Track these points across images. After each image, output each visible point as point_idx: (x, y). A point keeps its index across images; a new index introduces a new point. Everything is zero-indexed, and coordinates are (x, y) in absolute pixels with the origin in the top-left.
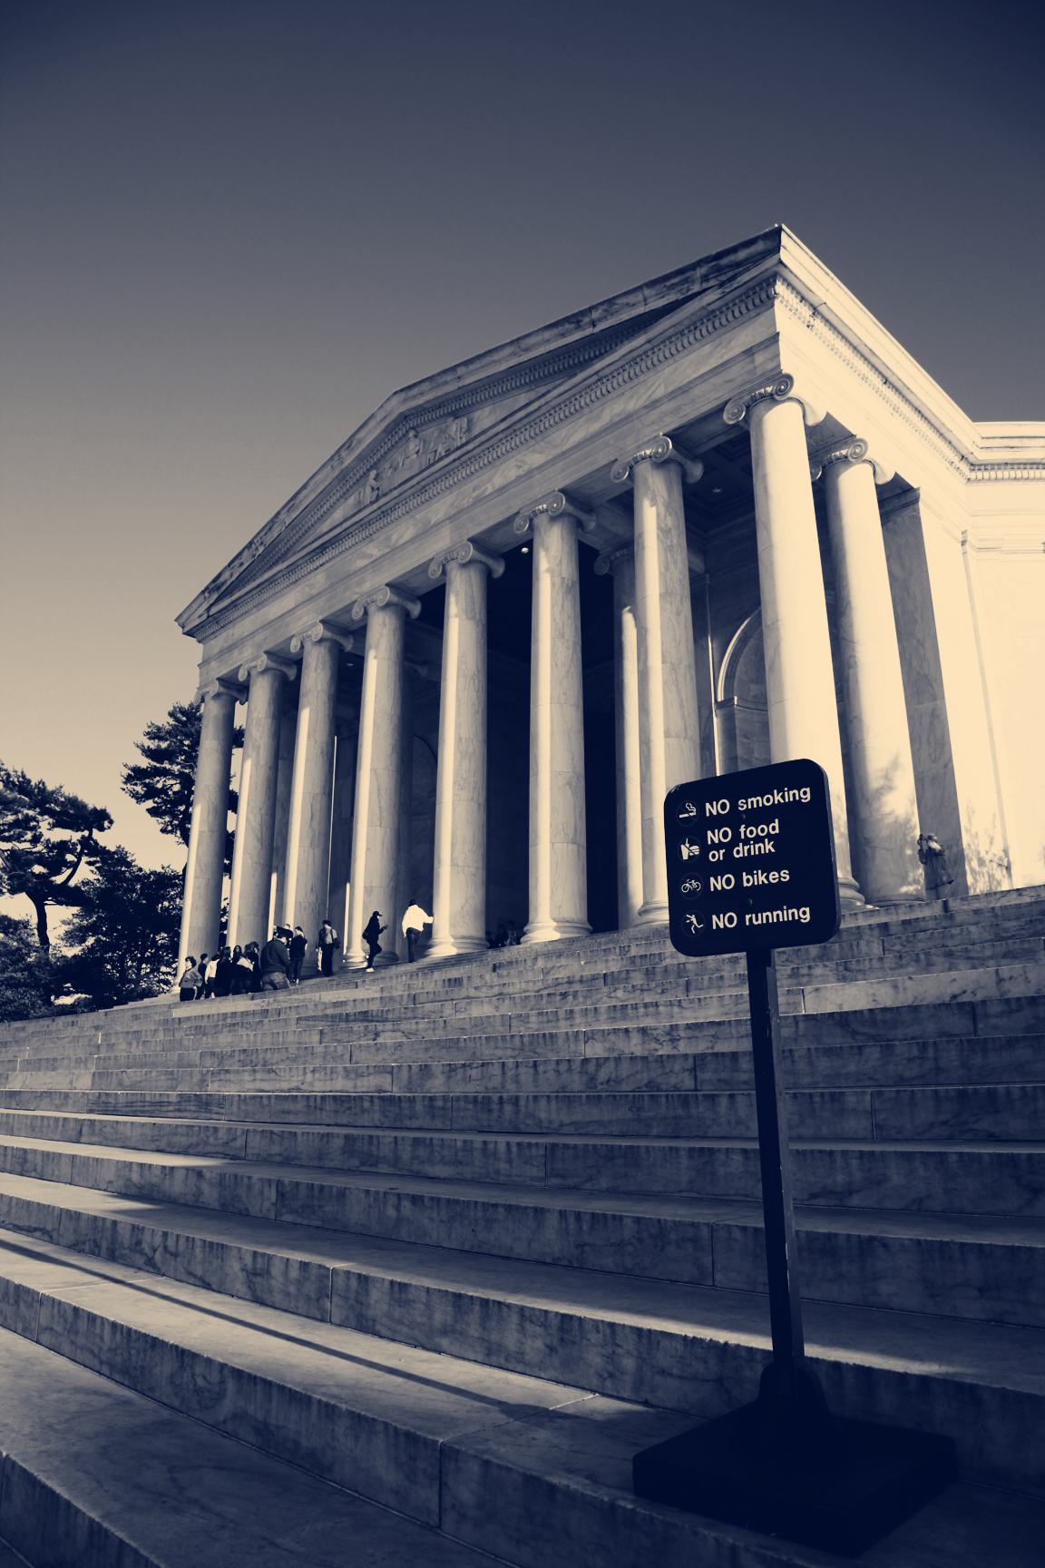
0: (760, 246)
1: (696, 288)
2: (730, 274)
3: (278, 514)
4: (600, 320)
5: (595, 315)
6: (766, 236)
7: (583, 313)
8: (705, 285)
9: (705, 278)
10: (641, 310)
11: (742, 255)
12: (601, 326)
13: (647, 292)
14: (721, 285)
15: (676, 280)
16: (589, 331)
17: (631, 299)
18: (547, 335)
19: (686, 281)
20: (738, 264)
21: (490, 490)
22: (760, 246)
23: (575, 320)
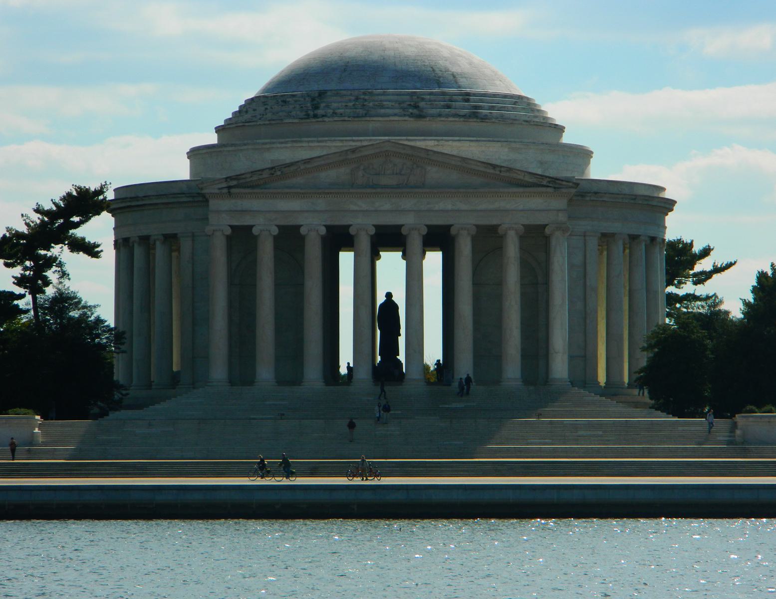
0: (571, 184)
1: (545, 183)
2: (557, 186)
3: (298, 162)
4: (504, 171)
5: (502, 169)
6: (574, 183)
7: (497, 166)
8: (548, 184)
9: (549, 182)
10: (521, 177)
11: (564, 183)
12: (502, 174)
13: (526, 174)
14: (555, 188)
15: (538, 177)
16: (498, 173)
17: (519, 172)
18: (479, 164)
19: (543, 179)
20: (562, 185)
21: (437, 208)
22: (571, 184)
23: (494, 166)
